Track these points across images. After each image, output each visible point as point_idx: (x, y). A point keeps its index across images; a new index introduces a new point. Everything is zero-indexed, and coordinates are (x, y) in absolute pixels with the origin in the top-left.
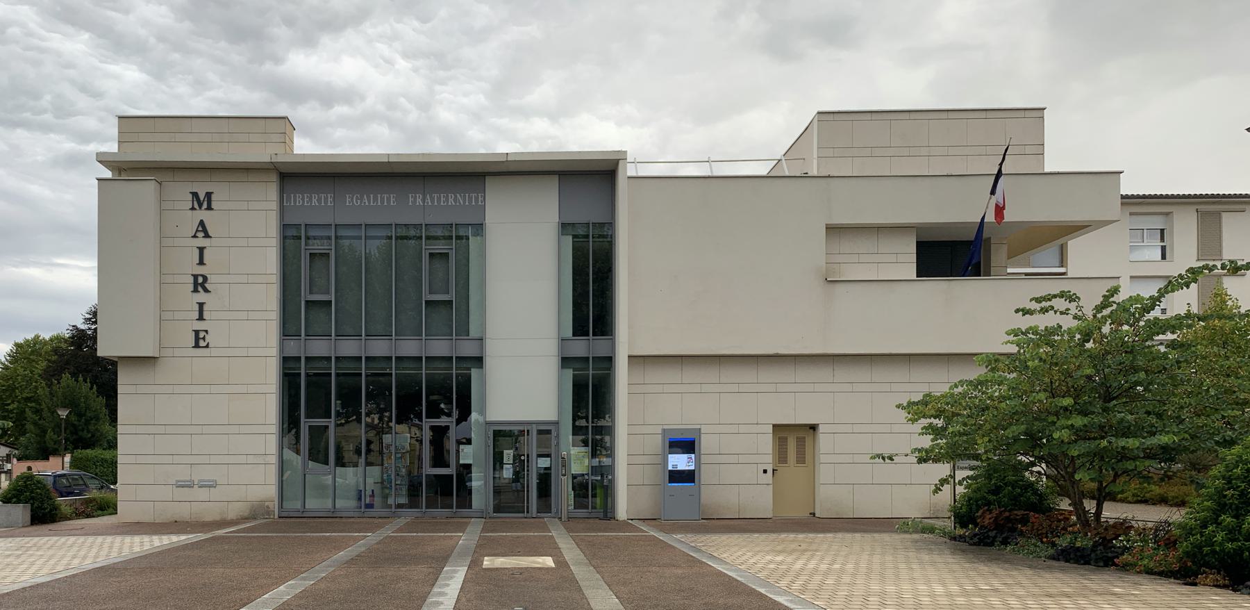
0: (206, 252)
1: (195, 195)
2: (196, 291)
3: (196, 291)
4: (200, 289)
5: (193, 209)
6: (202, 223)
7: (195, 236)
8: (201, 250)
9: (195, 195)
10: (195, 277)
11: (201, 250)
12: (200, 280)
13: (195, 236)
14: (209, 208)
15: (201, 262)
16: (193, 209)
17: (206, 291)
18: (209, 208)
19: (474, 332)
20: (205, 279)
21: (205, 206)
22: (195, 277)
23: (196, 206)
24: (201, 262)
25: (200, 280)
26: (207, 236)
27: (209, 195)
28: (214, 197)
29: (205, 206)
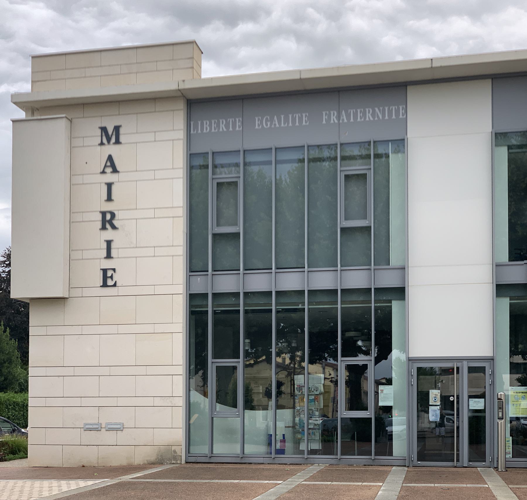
0: (114, 188)
1: (104, 130)
2: (104, 228)
3: (104, 228)
4: (108, 226)
5: (102, 144)
6: (110, 158)
7: (103, 172)
8: (109, 186)
9: (104, 130)
10: (104, 214)
11: (109, 186)
12: (108, 217)
13: (103, 172)
14: (118, 142)
15: (109, 198)
16: (102, 144)
17: (114, 227)
18: (118, 142)
19: (395, 260)
20: (113, 215)
21: (113, 140)
22: (104, 214)
23: (105, 141)
24: (109, 198)
25: (108, 217)
26: (115, 171)
27: (117, 129)
28: (122, 131)
29: (113, 140)
